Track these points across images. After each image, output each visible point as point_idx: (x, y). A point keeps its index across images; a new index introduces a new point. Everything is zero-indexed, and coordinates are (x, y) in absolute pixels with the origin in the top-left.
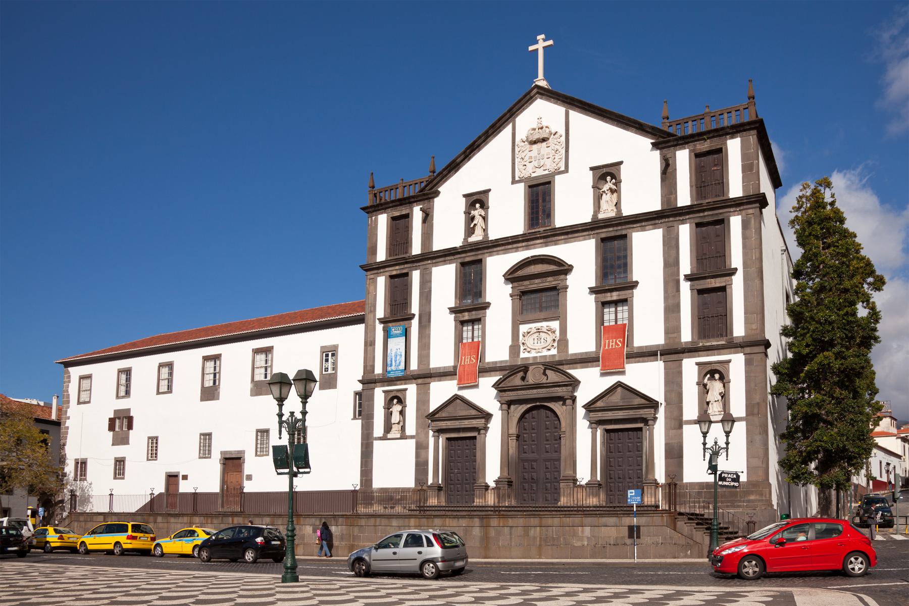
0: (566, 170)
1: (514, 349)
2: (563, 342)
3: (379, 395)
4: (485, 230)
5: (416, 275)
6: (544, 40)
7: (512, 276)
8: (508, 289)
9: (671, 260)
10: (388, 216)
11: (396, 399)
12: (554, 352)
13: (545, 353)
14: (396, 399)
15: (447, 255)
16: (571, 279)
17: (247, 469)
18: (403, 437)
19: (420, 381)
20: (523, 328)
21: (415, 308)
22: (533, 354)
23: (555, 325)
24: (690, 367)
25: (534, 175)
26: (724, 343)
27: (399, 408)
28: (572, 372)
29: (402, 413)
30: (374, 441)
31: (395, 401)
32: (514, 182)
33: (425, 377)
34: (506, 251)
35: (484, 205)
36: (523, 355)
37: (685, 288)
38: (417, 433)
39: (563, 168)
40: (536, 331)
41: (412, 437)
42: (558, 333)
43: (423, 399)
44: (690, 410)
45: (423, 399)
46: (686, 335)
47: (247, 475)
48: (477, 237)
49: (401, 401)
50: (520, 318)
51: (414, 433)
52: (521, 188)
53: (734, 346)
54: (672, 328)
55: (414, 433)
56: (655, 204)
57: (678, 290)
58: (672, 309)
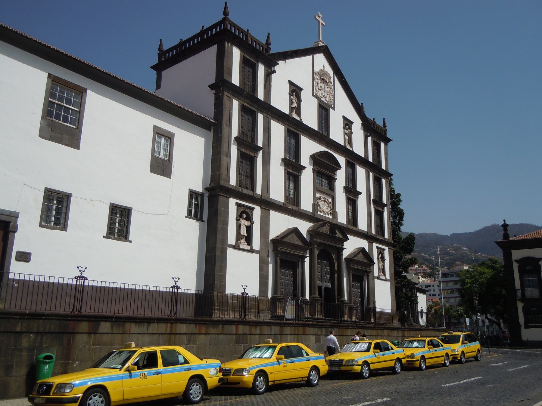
1: (315, 206)
2: (334, 213)
12: (330, 217)
13: (327, 216)
18: (252, 251)
22: (322, 214)
26: (383, 239)
27: (248, 223)
29: (249, 229)
40: (324, 199)
49: (249, 218)
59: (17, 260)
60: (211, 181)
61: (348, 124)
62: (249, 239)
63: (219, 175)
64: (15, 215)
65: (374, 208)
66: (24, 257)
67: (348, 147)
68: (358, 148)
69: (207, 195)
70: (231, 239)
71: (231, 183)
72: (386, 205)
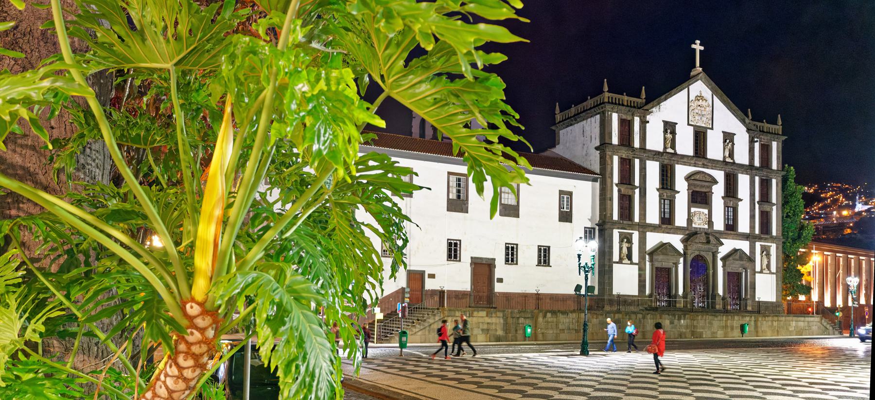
0: (712, 129)
1: (690, 221)
2: (710, 223)
3: (616, 234)
4: (673, 147)
5: (637, 161)
6: (700, 50)
7: (688, 178)
8: (686, 184)
9: (752, 193)
10: (618, 115)
11: (626, 239)
12: (706, 226)
13: (702, 226)
14: (626, 239)
15: (655, 155)
16: (715, 188)
17: (498, 273)
18: (632, 263)
19: (641, 230)
20: (693, 210)
21: (637, 183)
23: (706, 211)
24: (758, 245)
25: (698, 124)
28: (722, 240)
29: (630, 250)
30: (614, 264)
31: (625, 240)
32: (689, 124)
33: (644, 228)
34: (685, 164)
35: (673, 133)
36: (694, 225)
37: (757, 206)
38: (639, 262)
39: (711, 127)
41: (636, 264)
42: (707, 216)
43: (643, 241)
44: (758, 269)
45: (643, 241)
46: (757, 231)
47: (497, 279)
48: (670, 150)
49: (630, 241)
50: (691, 204)
51: (637, 262)
52: (690, 131)
53: (773, 239)
54: (752, 227)
55: (637, 262)
56: (746, 161)
57: (755, 209)
58: (752, 217)
59: (497, 282)
60: (600, 219)
61: (728, 137)
62: (629, 257)
63: (605, 215)
64: (494, 260)
65: (759, 209)
66: (500, 280)
67: (729, 160)
68: (741, 156)
69: (597, 228)
70: (616, 257)
71: (614, 219)
72: (774, 204)
